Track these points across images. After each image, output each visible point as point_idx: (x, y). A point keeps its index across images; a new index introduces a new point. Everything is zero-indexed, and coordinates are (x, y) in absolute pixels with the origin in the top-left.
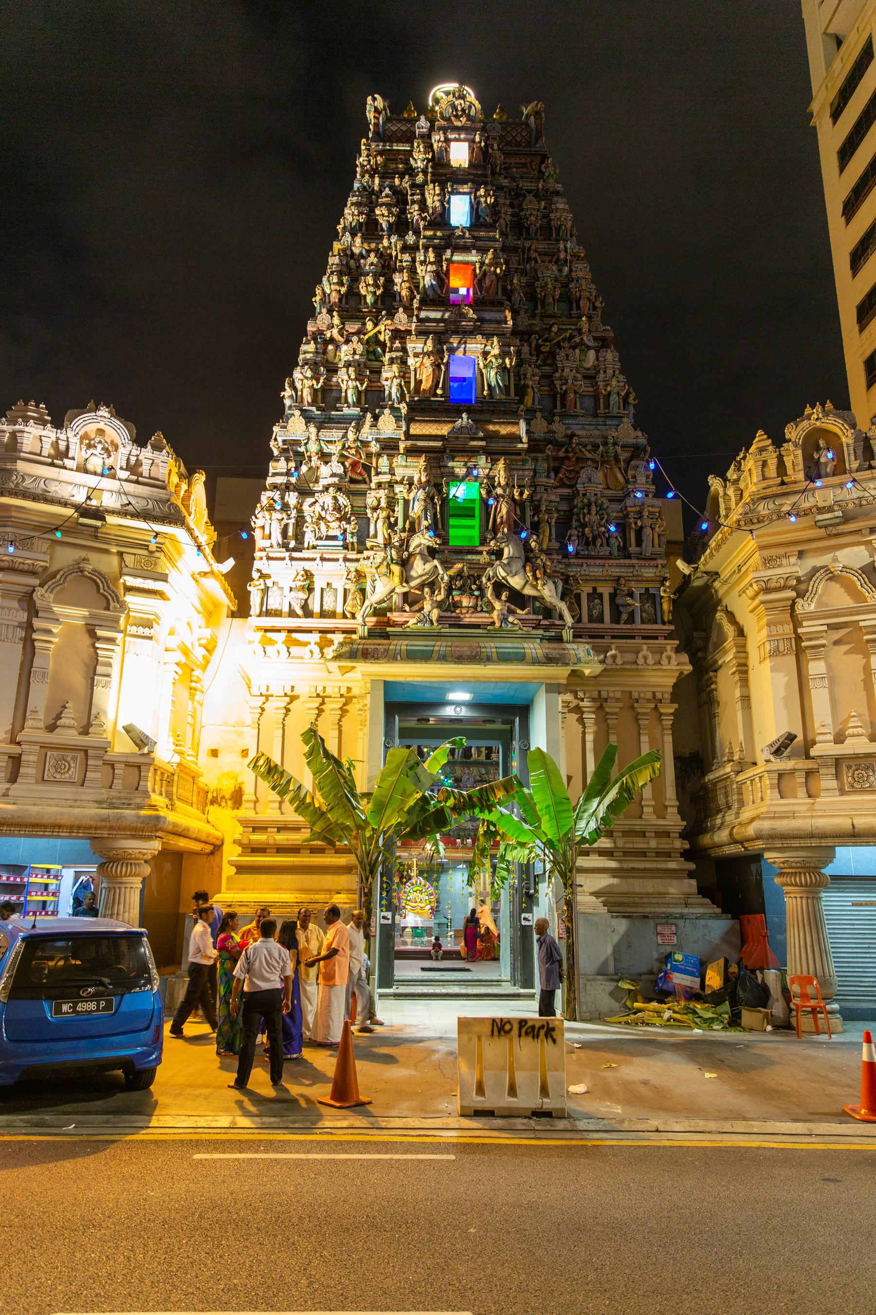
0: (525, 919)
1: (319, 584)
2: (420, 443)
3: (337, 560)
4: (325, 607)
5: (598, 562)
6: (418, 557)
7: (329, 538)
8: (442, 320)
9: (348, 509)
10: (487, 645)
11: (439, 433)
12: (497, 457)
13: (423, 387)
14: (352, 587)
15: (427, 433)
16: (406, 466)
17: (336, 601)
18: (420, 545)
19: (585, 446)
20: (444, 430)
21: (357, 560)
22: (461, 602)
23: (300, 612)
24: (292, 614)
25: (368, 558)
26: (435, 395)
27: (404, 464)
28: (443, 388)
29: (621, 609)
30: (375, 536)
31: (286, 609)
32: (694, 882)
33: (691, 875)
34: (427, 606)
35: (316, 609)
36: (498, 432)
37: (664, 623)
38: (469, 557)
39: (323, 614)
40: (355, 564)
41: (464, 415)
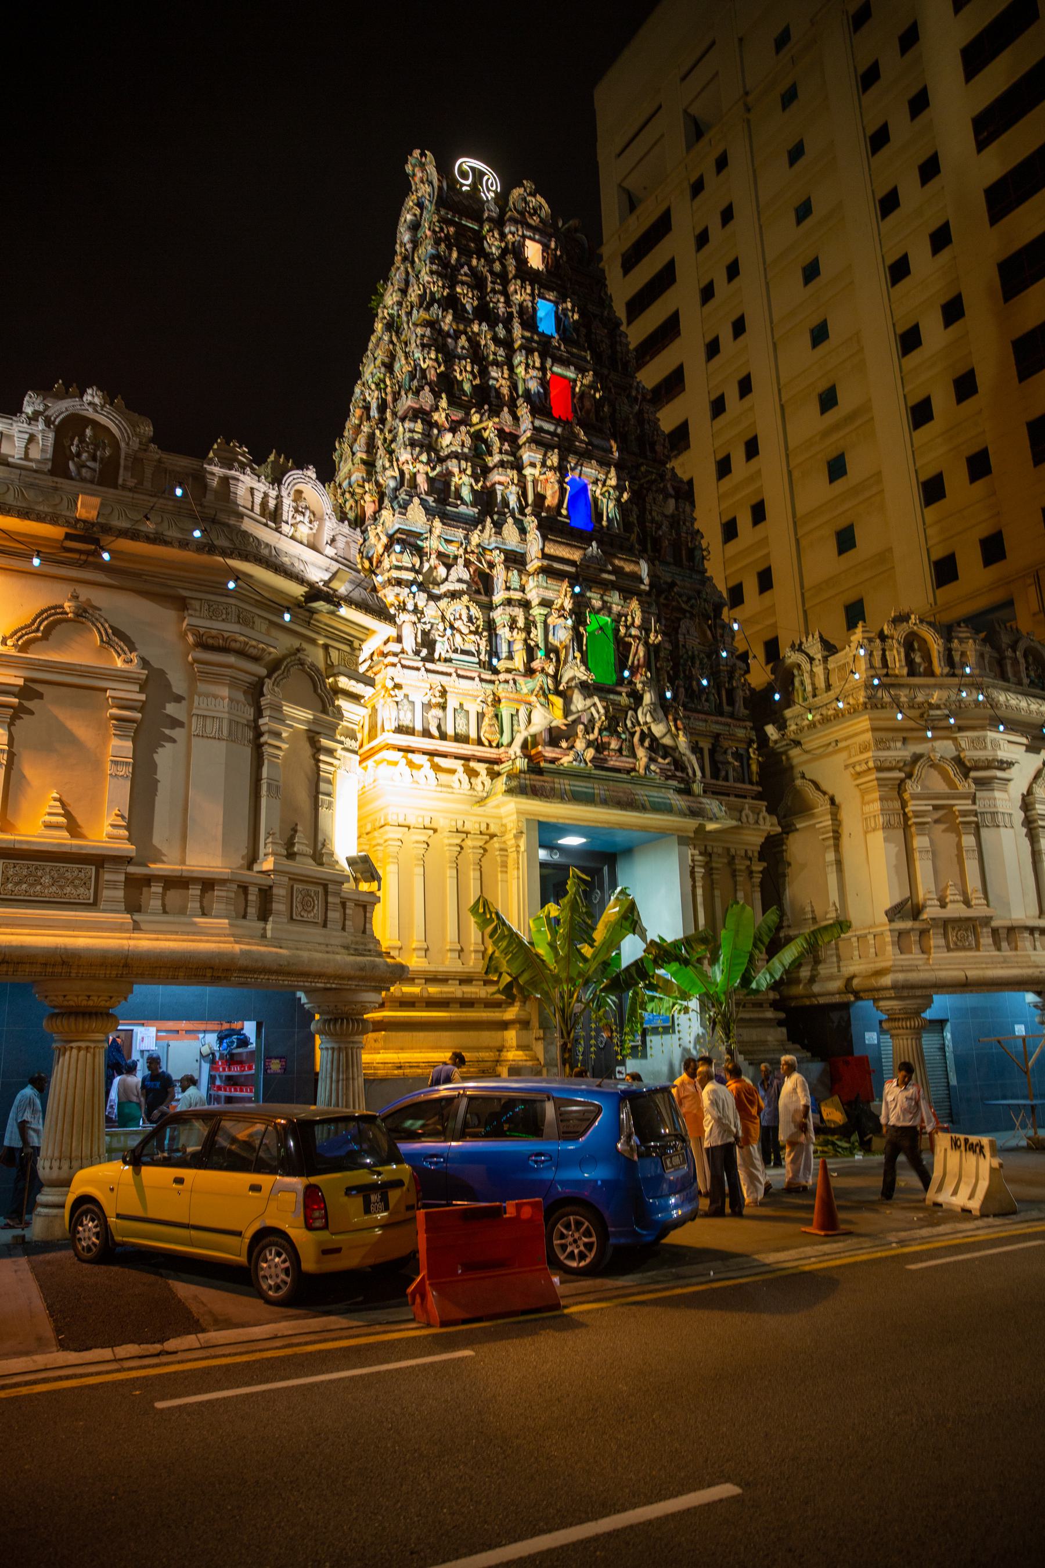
0: (620, 1072)
1: (452, 703)
2: (556, 565)
3: (473, 679)
4: (458, 731)
5: (701, 716)
6: (576, 691)
7: (464, 652)
8: (554, 434)
9: (480, 623)
10: (639, 792)
11: (571, 557)
12: (628, 595)
13: (547, 503)
14: (489, 711)
15: (560, 555)
16: (546, 588)
17: (468, 724)
18: (573, 678)
19: (680, 596)
20: (576, 555)
21: (492, 682)
22: (609, 744)
23: (435, 732)
24: (426, 733)
25: (507, 682)
26: (561, 515)
27: (545, 585)
28: (568, 509)
29: (720, 766)
30: (510, 657)
31: (419, 727)
32: (784, 1030)
33: (780, 1023)
34: (580, 745)
35: (450, 732)
36: (623, 568)
37: (751, 783)
38: (612, 696)
39: (459, 738)
40: (491, 686)
41: (594, 544)
